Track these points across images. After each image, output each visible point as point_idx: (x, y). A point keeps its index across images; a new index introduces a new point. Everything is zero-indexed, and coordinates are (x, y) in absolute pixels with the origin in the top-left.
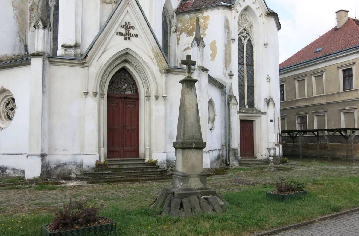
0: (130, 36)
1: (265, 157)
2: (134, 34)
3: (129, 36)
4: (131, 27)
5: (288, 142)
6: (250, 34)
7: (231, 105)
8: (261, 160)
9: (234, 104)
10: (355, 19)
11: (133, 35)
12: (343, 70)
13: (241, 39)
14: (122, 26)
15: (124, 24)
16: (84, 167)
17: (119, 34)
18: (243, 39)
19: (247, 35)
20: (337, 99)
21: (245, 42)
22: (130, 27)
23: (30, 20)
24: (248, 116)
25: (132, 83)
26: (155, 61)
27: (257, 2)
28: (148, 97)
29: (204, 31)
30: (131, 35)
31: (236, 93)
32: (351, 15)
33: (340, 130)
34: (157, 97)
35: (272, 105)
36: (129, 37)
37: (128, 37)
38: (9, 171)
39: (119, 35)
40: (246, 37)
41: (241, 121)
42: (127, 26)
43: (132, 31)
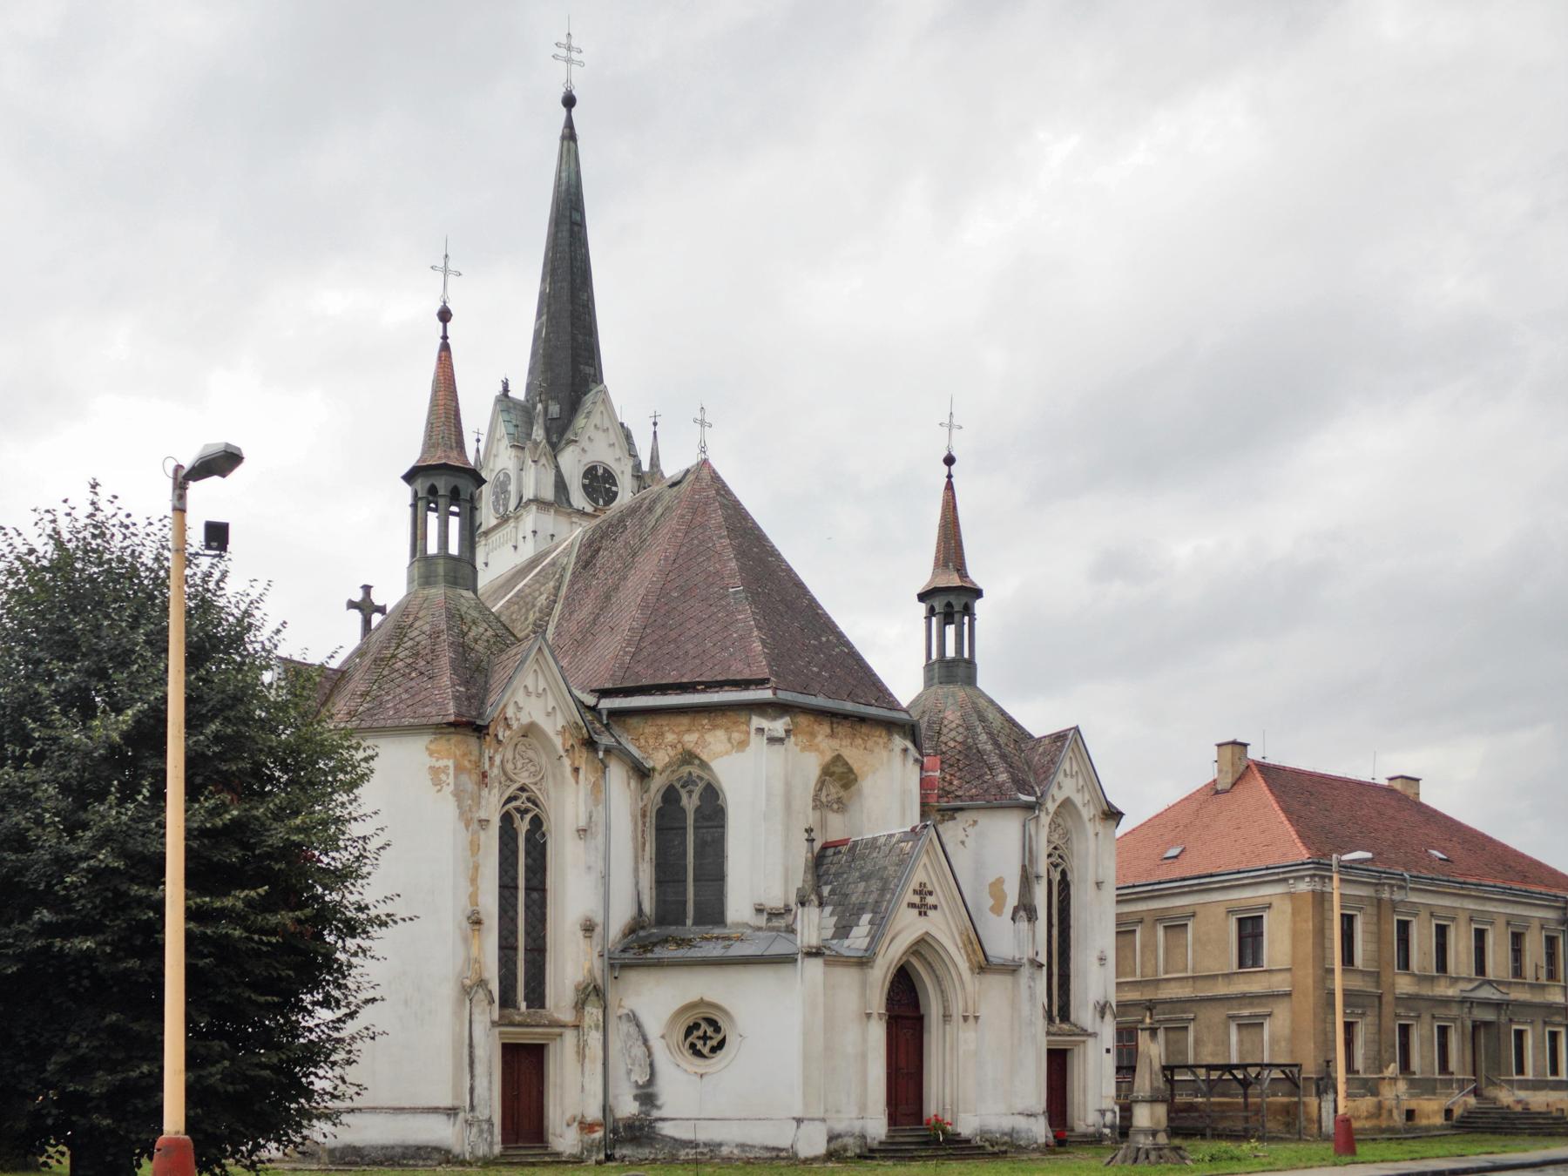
6: (1066, 858)
8: (1085, 1135)
10: (1262, 760)
12: (1240, 920)
14: (915, 892)
15: (918, 888)
16: (869, 1140)
20: (1222, 989)
24: (1060, 1042)
26: (963, 951)
27: (1085, 789)
28: (946, 1017)
32: (1254, 754)
33: (1229, 1068)
34: (965, 1018)
38: (730, 1149)
43: (930, 900)
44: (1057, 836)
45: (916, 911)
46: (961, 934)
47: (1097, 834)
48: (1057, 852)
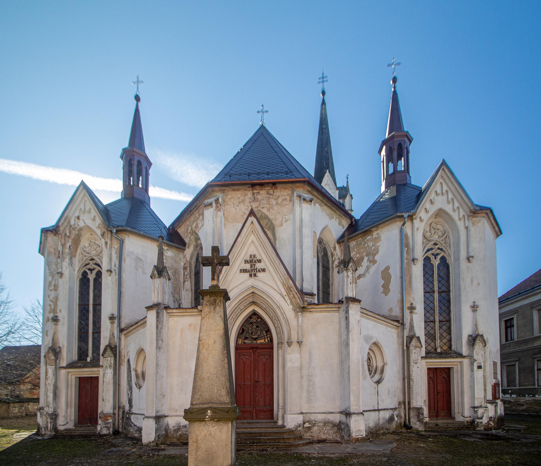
0: (257, 272)
1: (468, 419)
2: (261, 269)
3: (254, 272)
4: (257, 260)
5: (520, 397)
7: (411, 348)
9: (416, 347)
11: (260, 270)
13: (429, 258)
14: (246, 262)
15: (249, 259)
17: (242, 271)
18: (432, 258)
19: (439, 251)
21: (436, 262)
22: (256, 261)
23: (184, 279)
25: (266, 330)
26: (287, 298)
28: (280, 343)
29: (374, 257)
30: (258, 270)
31: (420, 330)
35: (481, 344)
36: (255, 273)
37: (254, 274)
39: (243, 272)
40: (438, 254)
41: (428, 368)
42: (253, 259)
43: (259, 266)
44: (437, 237)
45: (247, 275)
46: (284, 285)
47: (467, 228)
48: (437, 247)
